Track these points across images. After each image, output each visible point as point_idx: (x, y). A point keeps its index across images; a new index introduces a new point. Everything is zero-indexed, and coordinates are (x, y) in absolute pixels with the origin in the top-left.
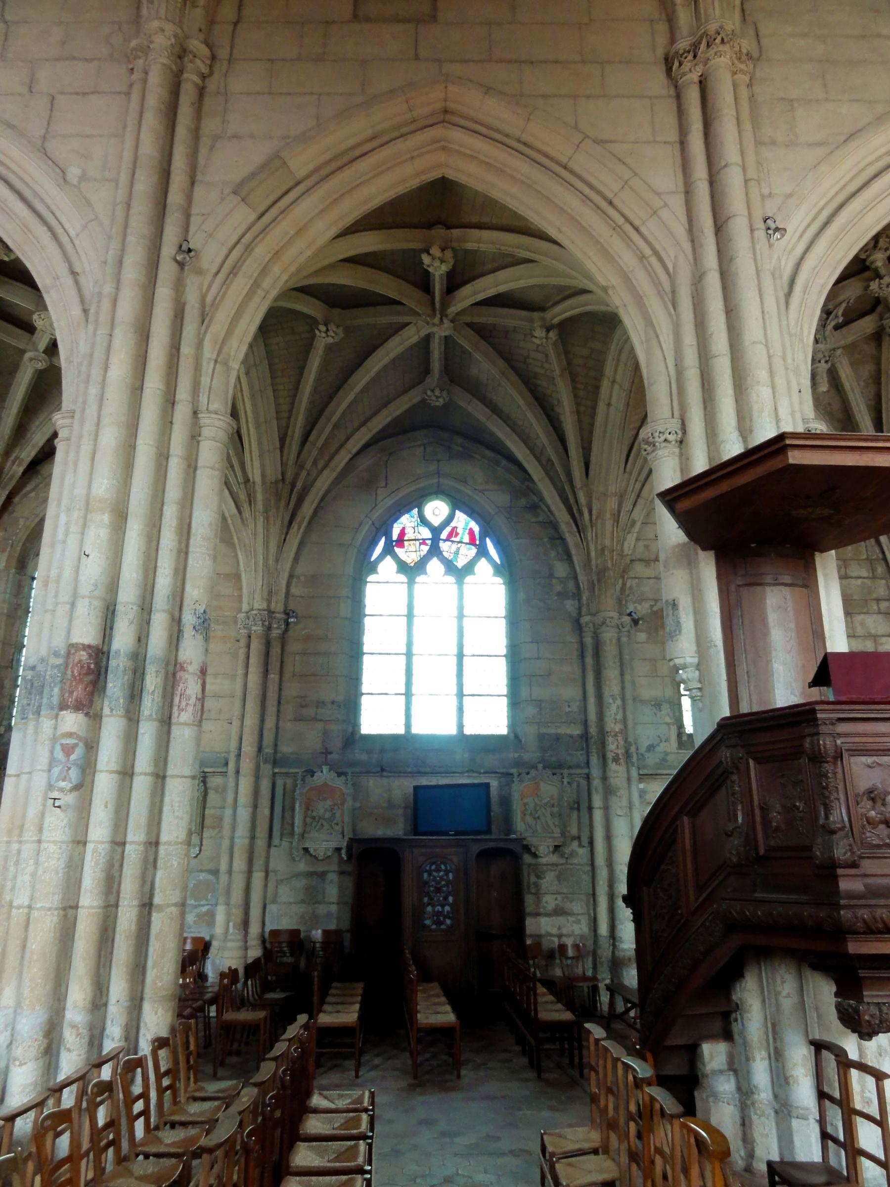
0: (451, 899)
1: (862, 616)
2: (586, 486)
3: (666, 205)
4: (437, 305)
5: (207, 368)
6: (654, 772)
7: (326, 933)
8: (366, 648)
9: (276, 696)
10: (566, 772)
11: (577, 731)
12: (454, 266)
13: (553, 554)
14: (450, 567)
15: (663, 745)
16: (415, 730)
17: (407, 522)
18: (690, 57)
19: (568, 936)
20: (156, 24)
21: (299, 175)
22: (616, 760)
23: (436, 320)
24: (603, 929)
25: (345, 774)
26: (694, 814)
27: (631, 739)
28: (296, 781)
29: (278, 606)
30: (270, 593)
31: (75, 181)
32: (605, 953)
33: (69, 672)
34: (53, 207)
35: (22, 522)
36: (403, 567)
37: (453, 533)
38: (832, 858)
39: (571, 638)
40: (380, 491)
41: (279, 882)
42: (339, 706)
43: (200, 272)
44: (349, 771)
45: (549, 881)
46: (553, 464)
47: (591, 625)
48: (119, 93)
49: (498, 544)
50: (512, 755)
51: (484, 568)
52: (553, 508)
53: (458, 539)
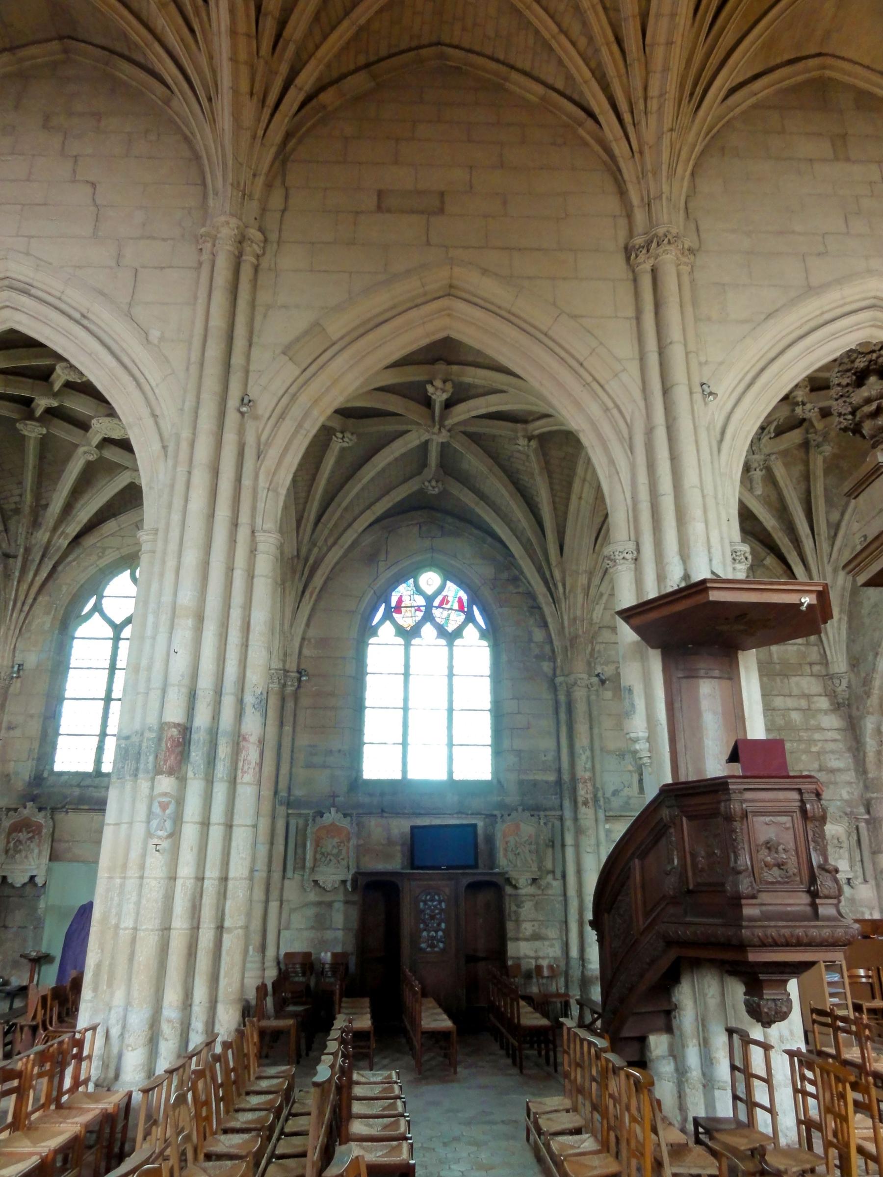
0: (443, 926)
1: (797, 678)
2: (561, 564)
3: (624, 370)
4: (437, 419)
5: (262, 494)
6: (618, 814)
7: (334, 955)
8: (367, 703)
9: (290, 745)
10: (542, 813)
11: (552, 777)
12: (452, 394)
13: (531, 621)
14: (442, 631)
15: (626, 790)
16: (411, 776)
17: (404, 591)
18: (644, 251)
19: (543, 958)
20: (222, 219)
21: (335, 338)
22: (585, 803)
23: (436, 430)
24: (574, 953)
25: (350, 815)
26: (643, 856)
27: (598, 785)
28: (307, 821)
29: (292, 665)
30: (285, 655)
31: (156, 342)
32: (575, 973)
33: (163, 745)
34: (137, 361)
35: (64, 588)
36: (401, 631)
37: (444, 601)
38: (738, 892)
39: (547, 696)
40: (381, 564)
41: (292, 911)
42: (345, 755)
43: (256, 418)
44: (354, 812)
45: (527, 910)
46: (532, 544)
47: (564, 685)
48: (190, 268)
49: (484, 611)
50: (496, 799)
52: (532, 582)
53: (448, 606)
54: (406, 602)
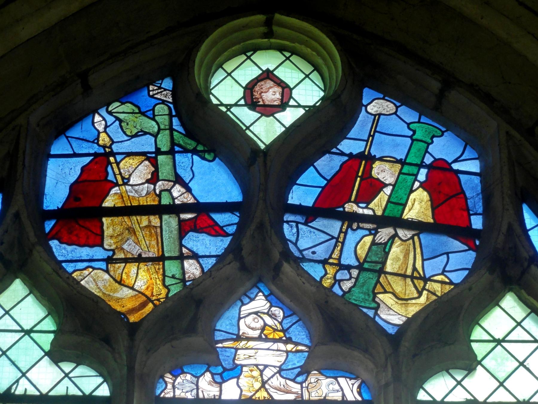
14: (336, 331)
37: (355, 178)
53: (378, 205)
54: (135, 179)
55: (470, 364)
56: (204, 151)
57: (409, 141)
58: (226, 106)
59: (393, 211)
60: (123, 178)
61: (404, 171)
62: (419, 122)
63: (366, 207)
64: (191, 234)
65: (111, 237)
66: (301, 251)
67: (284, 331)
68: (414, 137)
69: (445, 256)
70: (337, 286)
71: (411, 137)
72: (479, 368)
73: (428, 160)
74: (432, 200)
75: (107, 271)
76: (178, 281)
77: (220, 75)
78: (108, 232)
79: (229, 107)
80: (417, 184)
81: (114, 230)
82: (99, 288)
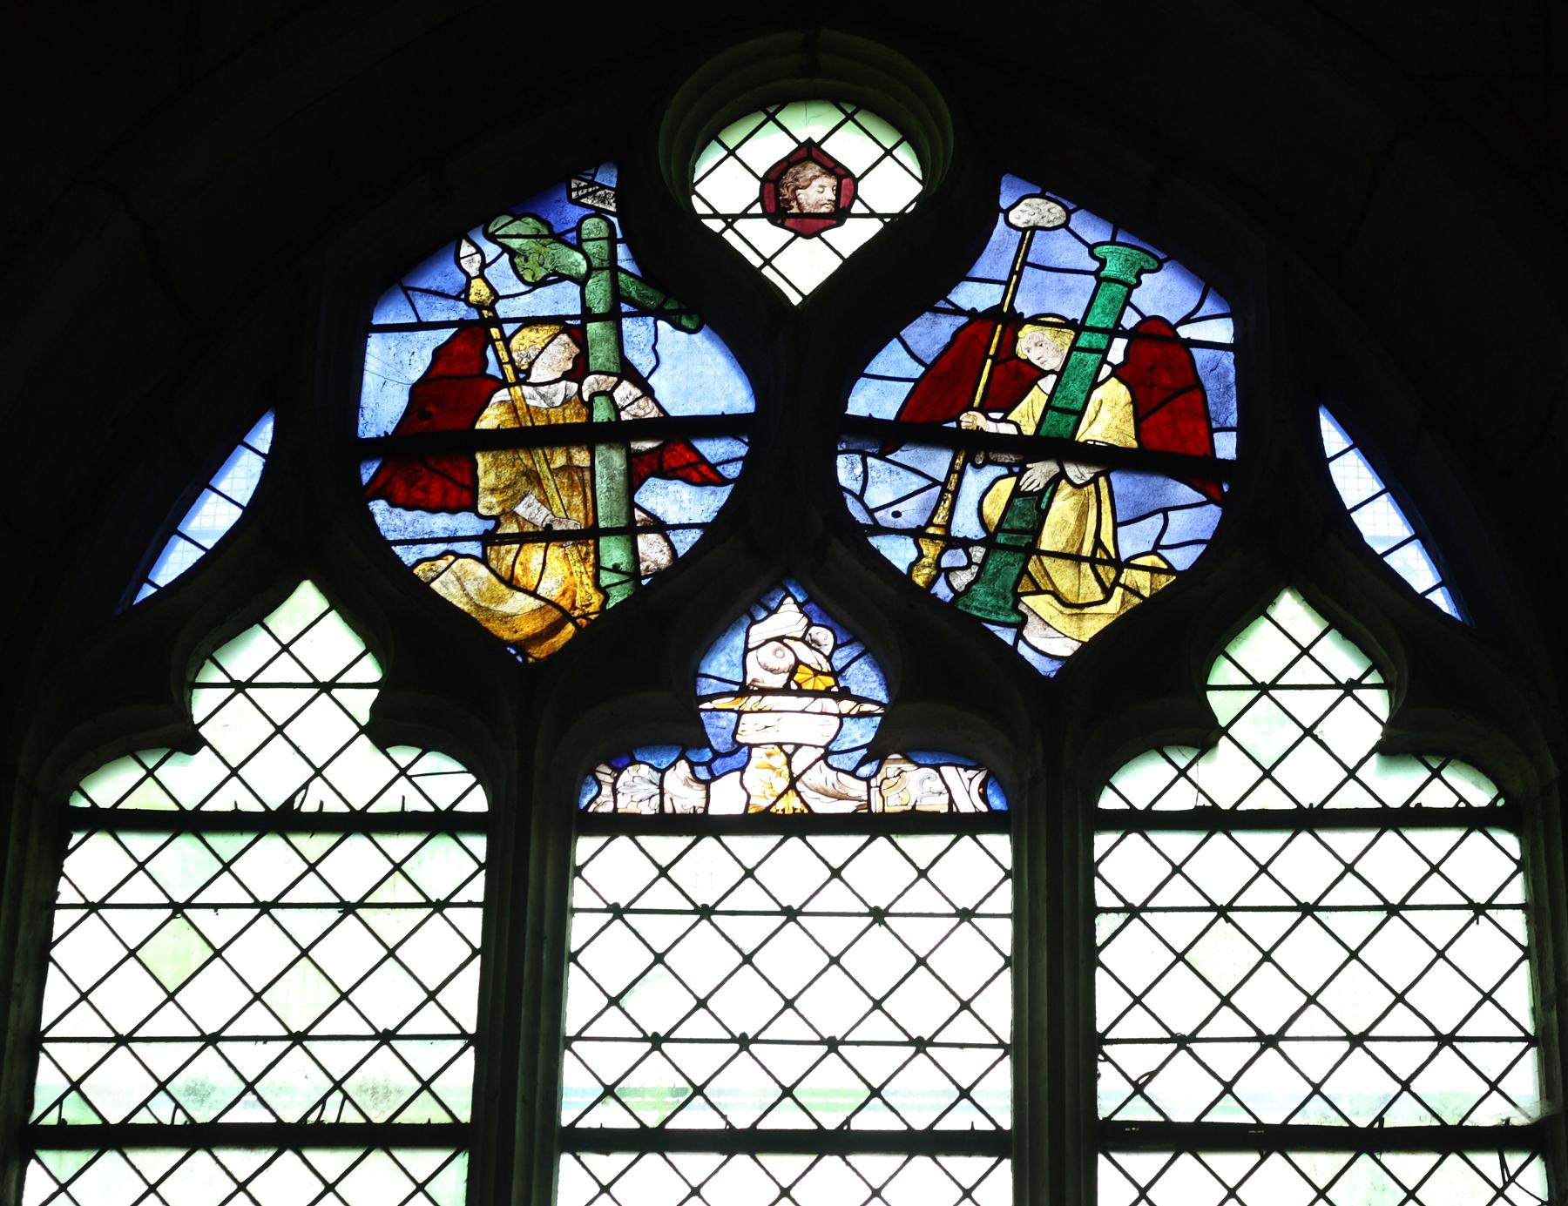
14: (940, 674)
36: (435, 678)
51: (1296, 697)
53: (1028, 414)
55: (1204, 734)
56: (680, 312)
57: (1091, 281)
58: (724, 217)
59: (1060, 425)
60: (517, 370)
61: (1082, 343)
62: (1113, 242)
63: (1004, 420)
64: (651, 481)
65: (493, 491)
66: (871, 512)
67: (835, 674)
68: (1103, 274)
69: (1160, 516)
70: (942, 580)
71: (1096, 274)
72: (1224, 741)
73: (1130, 320)
74: (1135, 401)
75: (484, 560)
76: (624, 578)
77: (714, 153)
78: (486, 480)
79: (730, 220)
80: (1106, 370)
81: (498, 477)
82: (467, 595)
